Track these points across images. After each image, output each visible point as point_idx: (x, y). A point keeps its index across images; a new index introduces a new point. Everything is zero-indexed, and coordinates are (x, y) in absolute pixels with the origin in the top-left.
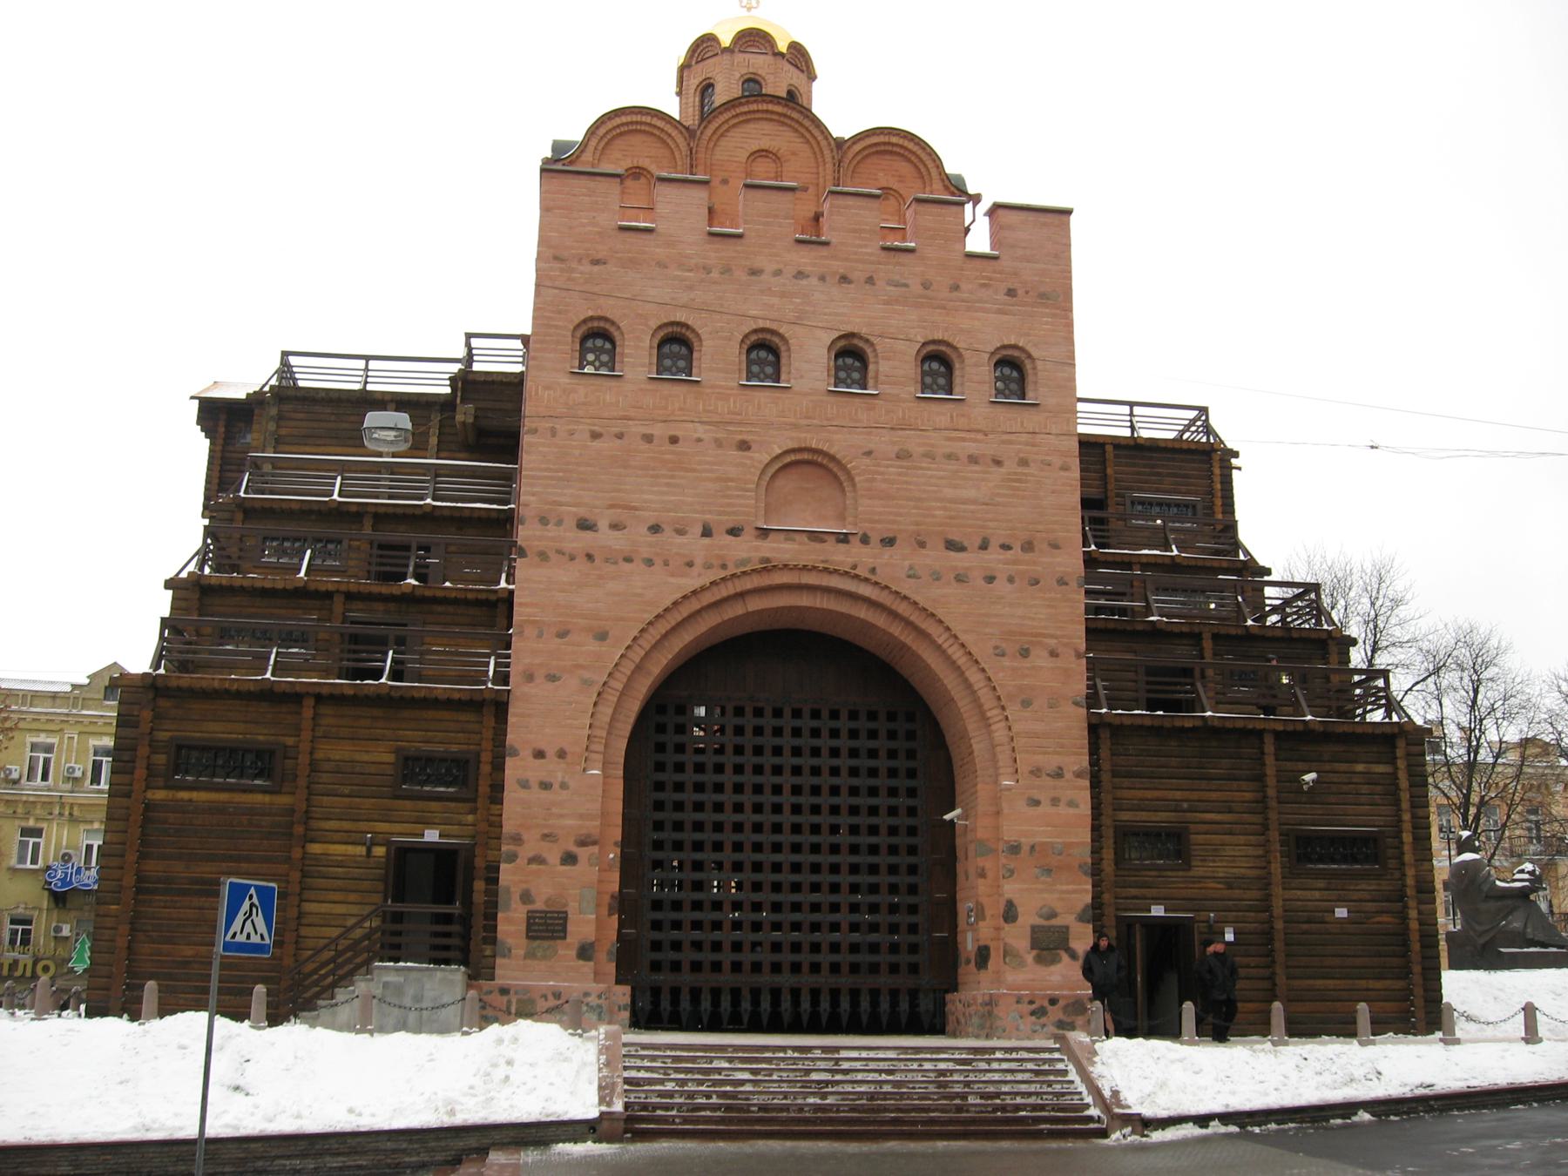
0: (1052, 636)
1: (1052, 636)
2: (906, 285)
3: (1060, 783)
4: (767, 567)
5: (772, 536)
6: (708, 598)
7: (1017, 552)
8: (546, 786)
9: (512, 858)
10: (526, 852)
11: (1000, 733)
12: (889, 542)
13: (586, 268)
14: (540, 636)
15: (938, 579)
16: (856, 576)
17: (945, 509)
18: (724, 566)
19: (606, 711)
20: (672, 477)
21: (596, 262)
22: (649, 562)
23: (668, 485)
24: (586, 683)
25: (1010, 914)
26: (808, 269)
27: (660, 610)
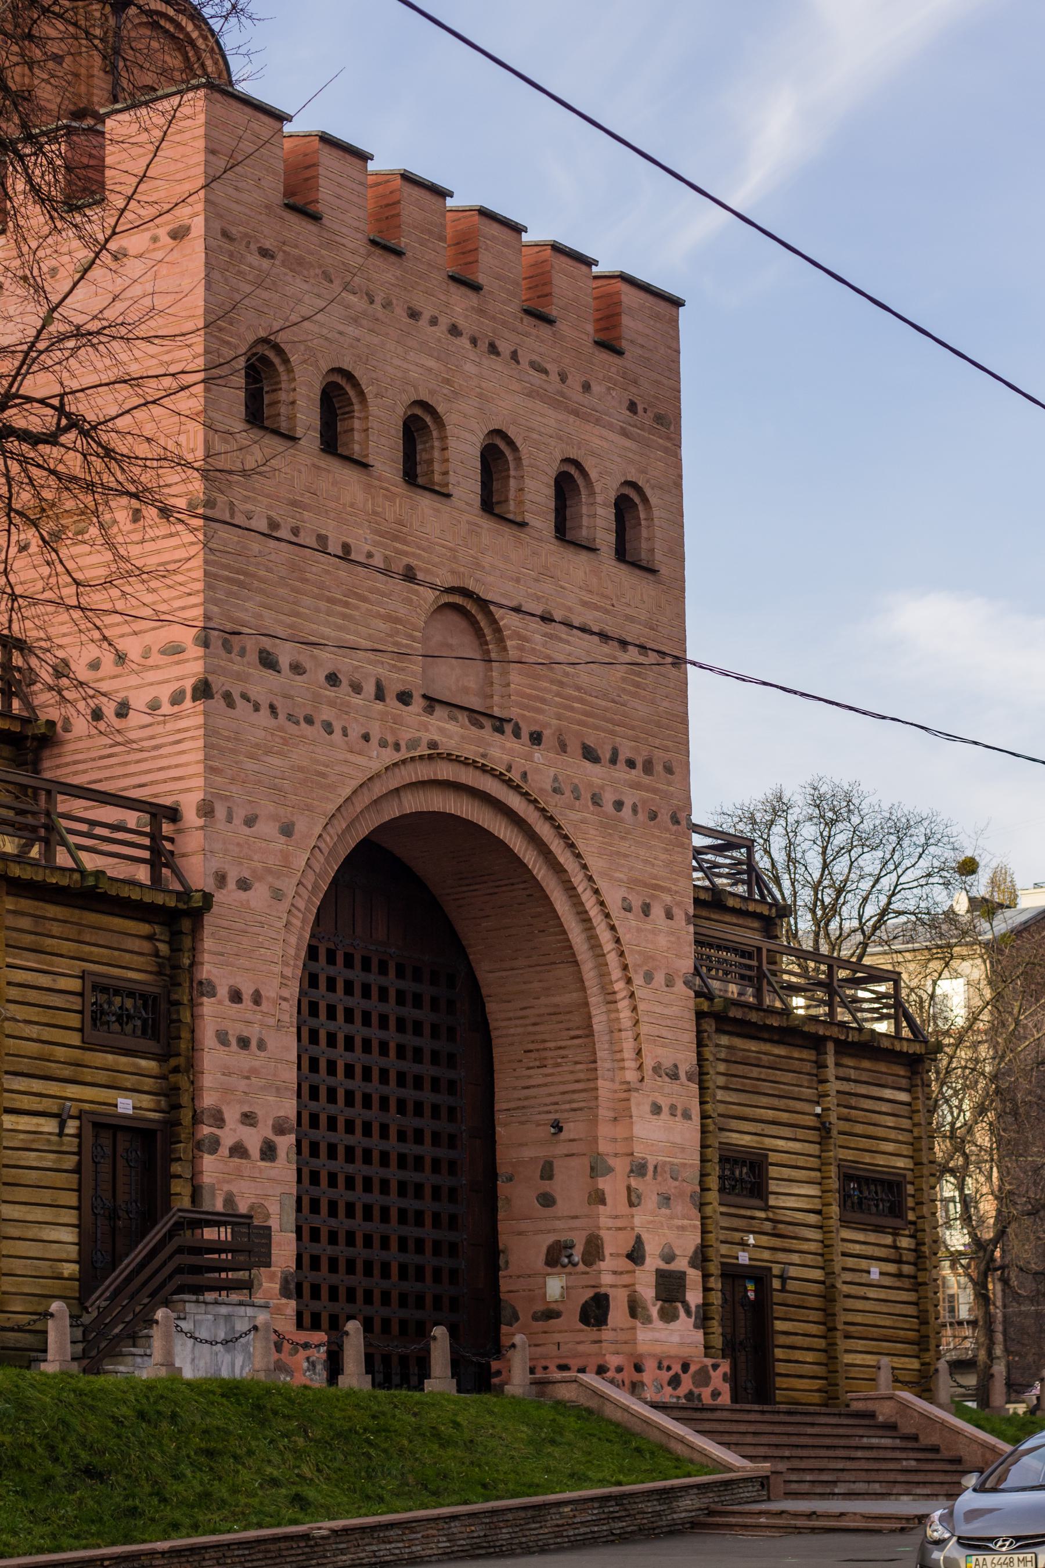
2: (546, 372)
3: (673, 1087)
4: (435, 755)
5: (440, 712)
6: (378, 789)
7: (636, 774)
8: (244, 1043)
9: (214, 1145)
10: (228, 1137)
11: (625, 1015)
12: (536, 738)
13: (255, 259)
14: (230, 819)
15: (577, 798)
16: (509, 783)
17: (582, 701)
18: (397, 747)
20: (346, 605)
21: (264, 253)
22: (328, 728)
23: (344, 617)
24: (277, 895)
25: (636, 1255)
26: (461, 323)
27: (341, 801)
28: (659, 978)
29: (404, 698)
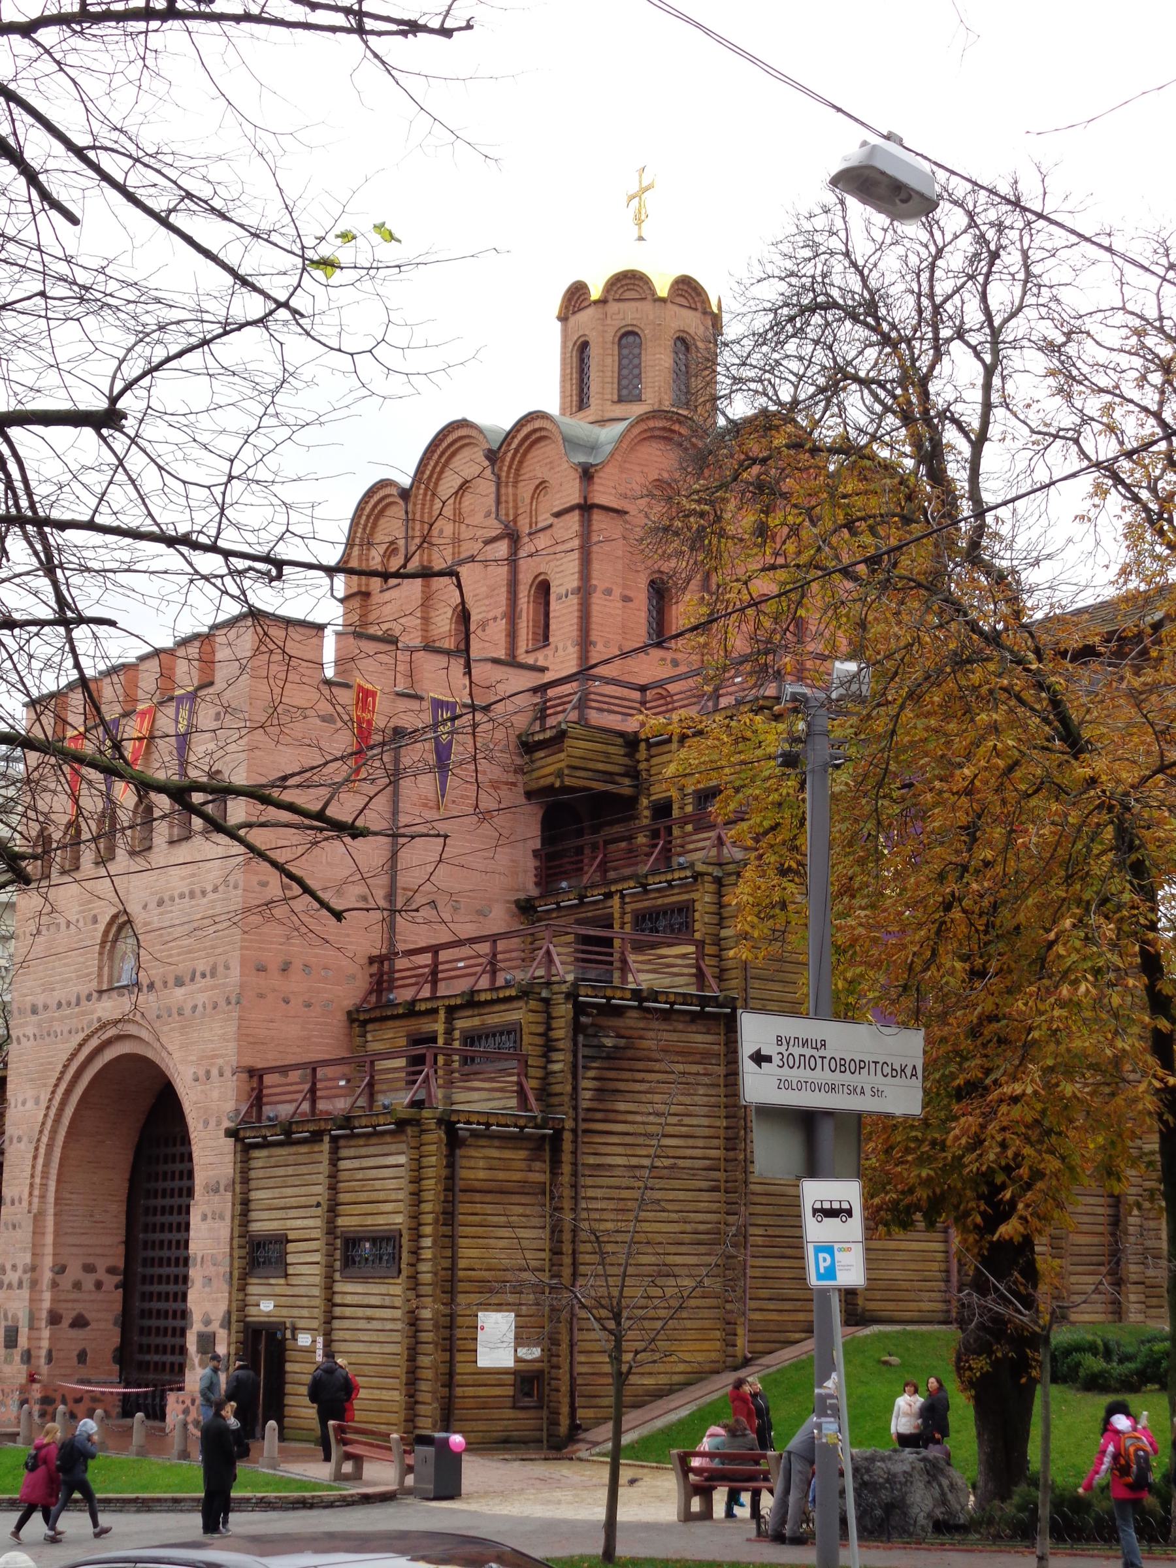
0: (221, 1056)
1: (221, 1056)
3: (217, 1198)
4: (103, 1026)
5: (105, 996)
19: (40, 1161)
28: (213, 1123)
29: (89, 997)
